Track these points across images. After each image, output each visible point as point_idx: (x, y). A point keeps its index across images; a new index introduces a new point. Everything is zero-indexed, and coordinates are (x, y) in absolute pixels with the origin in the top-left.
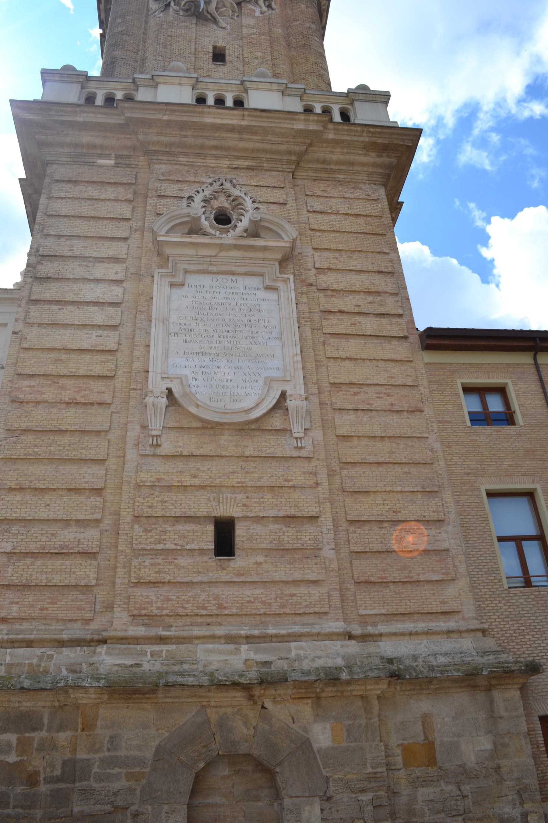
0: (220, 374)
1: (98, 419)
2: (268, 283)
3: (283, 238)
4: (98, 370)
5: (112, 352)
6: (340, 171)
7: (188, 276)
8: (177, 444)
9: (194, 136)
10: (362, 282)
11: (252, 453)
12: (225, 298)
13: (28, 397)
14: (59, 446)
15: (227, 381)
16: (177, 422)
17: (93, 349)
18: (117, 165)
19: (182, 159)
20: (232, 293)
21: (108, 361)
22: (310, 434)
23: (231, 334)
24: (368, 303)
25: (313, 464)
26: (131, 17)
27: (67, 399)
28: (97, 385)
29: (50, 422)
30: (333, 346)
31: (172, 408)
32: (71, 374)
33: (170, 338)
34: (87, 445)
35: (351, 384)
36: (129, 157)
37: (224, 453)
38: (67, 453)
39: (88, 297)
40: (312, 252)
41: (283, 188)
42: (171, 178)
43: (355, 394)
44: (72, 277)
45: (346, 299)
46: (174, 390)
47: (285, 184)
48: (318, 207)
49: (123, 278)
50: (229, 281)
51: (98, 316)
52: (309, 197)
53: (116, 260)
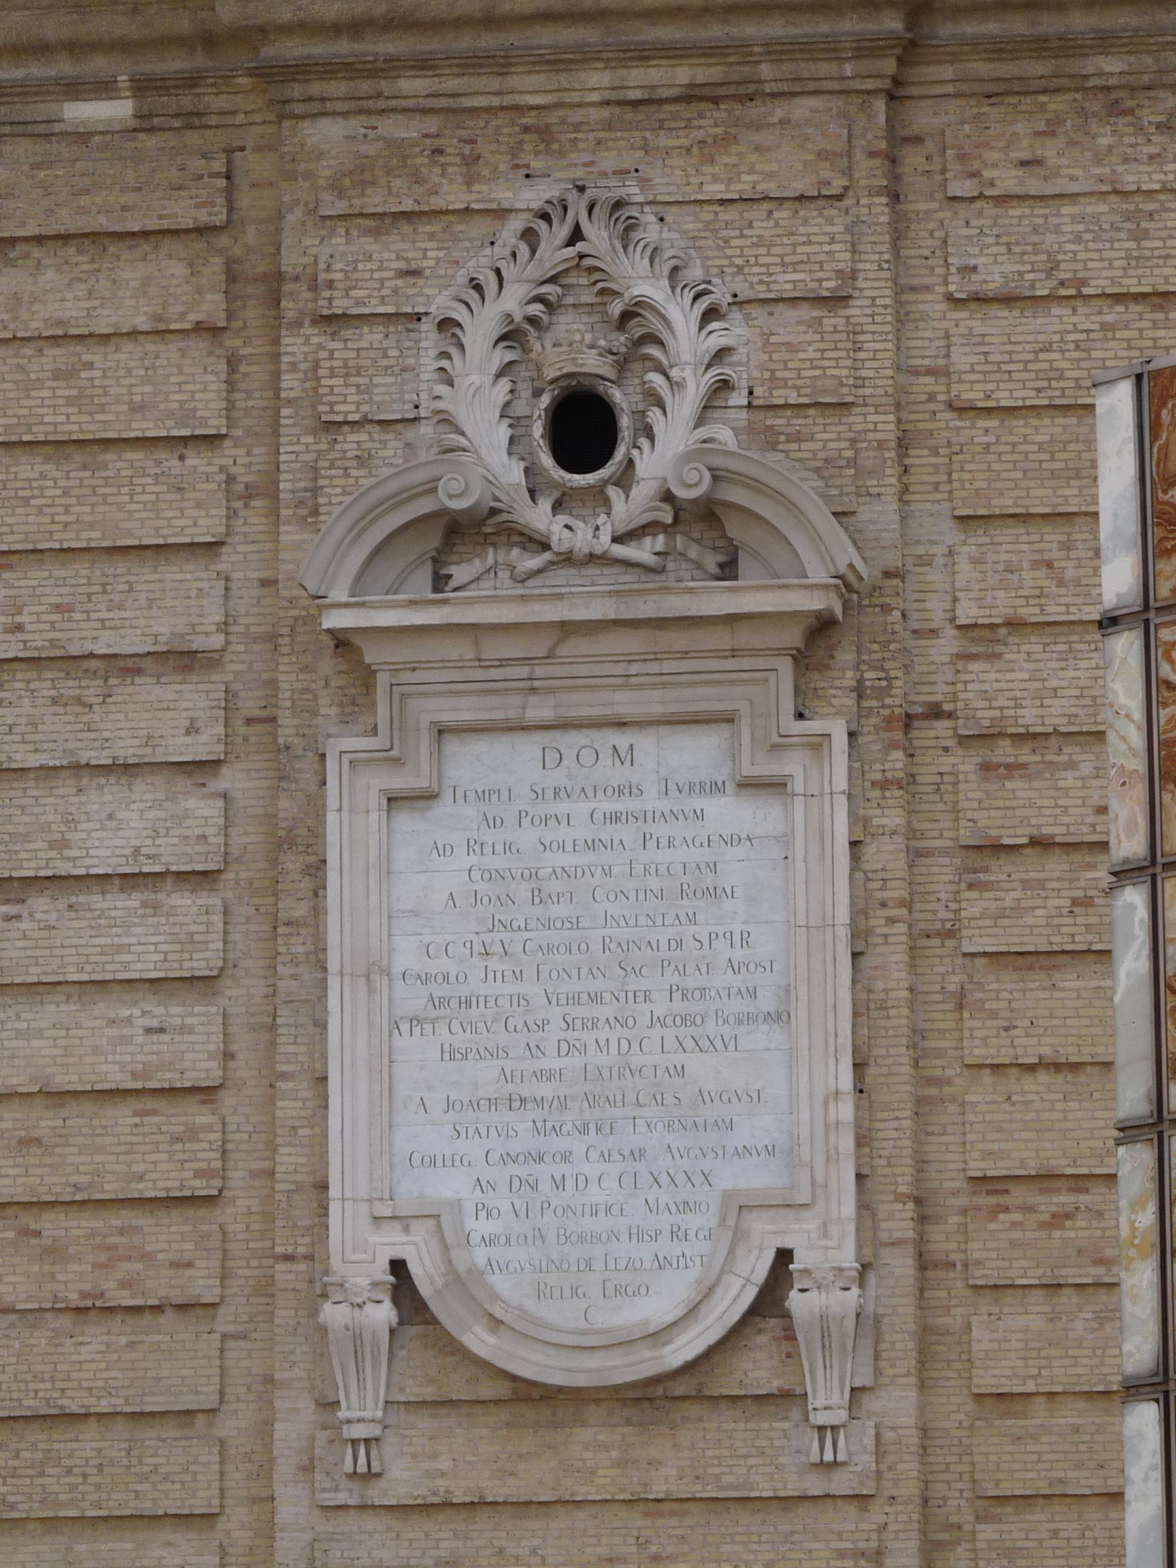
0: (570, 1183)
1: (179, 1365)
4: (167, 1179)
5: (205, 1093)
6: (1105, 42)
7: (452, 746)
8: (436, 1465)
11: (673, 1488)
12: (591, 845)
14: (69, 1472)
15: (594, 1213)
16: (431, 1381)
17: (139, 1085)
18: (145, 123)
19: (411, 85)
20: (615, 818)
21: (193, 1133)
22: (871, 1403)
23: (606, 1011)
25: (876, 1516)
27: (73, 1298)
28: (165, 1235)
29: (32, 1386)
30: (994, 1015)
31: (413, 1330)
32: (78, 1197)
33: (398, 1042)
34: (156, 1466)
35: (1047, 1179)
36: (191, 81)
37: (584, 1492)
38: (94, 1497)
39: (103, 852)
40: (951, 535)
42: (375, 201)
43: (1059, 1219)
44: (33, 761)
45: (1068, 780)
46: (414, 1268)
47: (849, 172)
48: (993, 275)
49: (217, 751)
50: (606, 758)
51: (143, 938)
52: (964, 210)
53: (183, 660)
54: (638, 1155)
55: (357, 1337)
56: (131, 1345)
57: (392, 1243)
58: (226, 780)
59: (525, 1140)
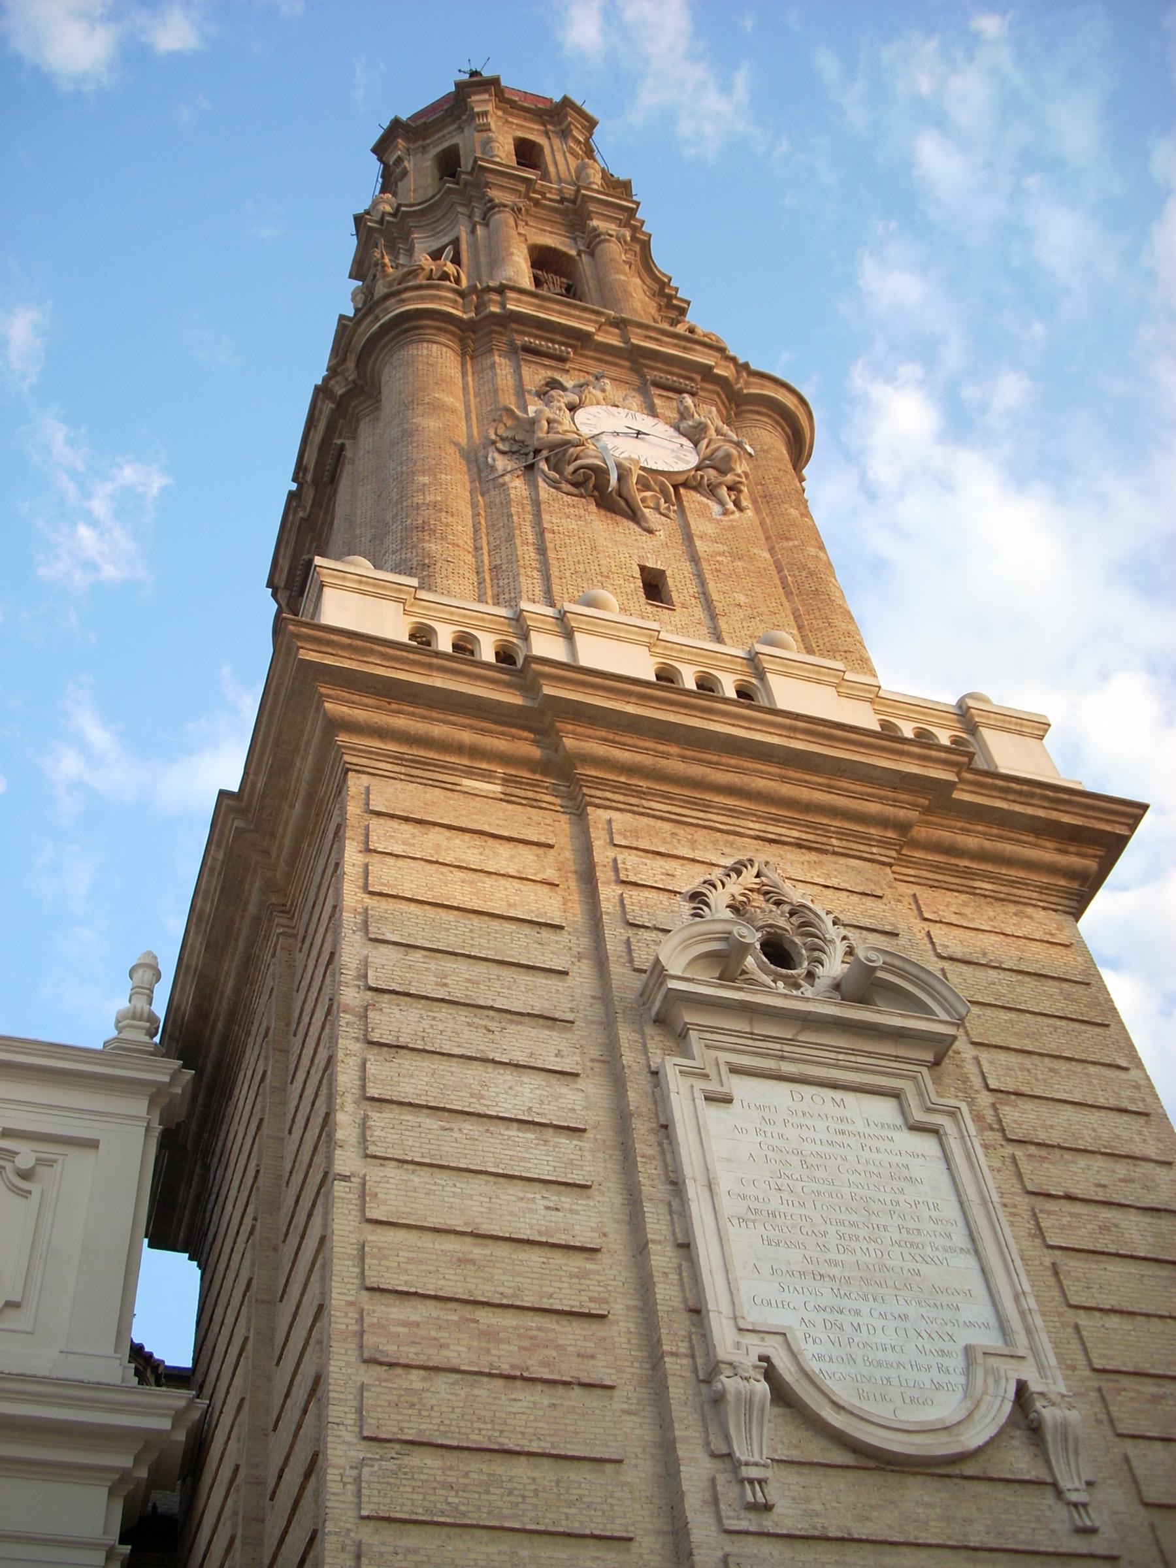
2: (919, 1116)
3: (931, 1012)
5: (590, 1251)
8: (810, 1507)
9: (683, 758)
10: (1094, 1130)
11: (985, 1540)
12: (831, 1144)
13: (410, 1354)
14: (510, 1493)
16: (796, 1447)
17: (544, 1240)
23: (863, 1233)
24: (1121, 1180)
26: (449, 477)
27: (506, 1369)
28: (572, 1334)
29: (476, 1425)
30: (1078, 1279)
32: (504, 1301)
34: (581, 1496)
38: (533, 1514)
41: (880, 897)
54: (904, 1318)
55: (749, 1402)
56: (553, 1406)
57: (756, 1346)
58: (581, 1083)
59: (827, 1299)
